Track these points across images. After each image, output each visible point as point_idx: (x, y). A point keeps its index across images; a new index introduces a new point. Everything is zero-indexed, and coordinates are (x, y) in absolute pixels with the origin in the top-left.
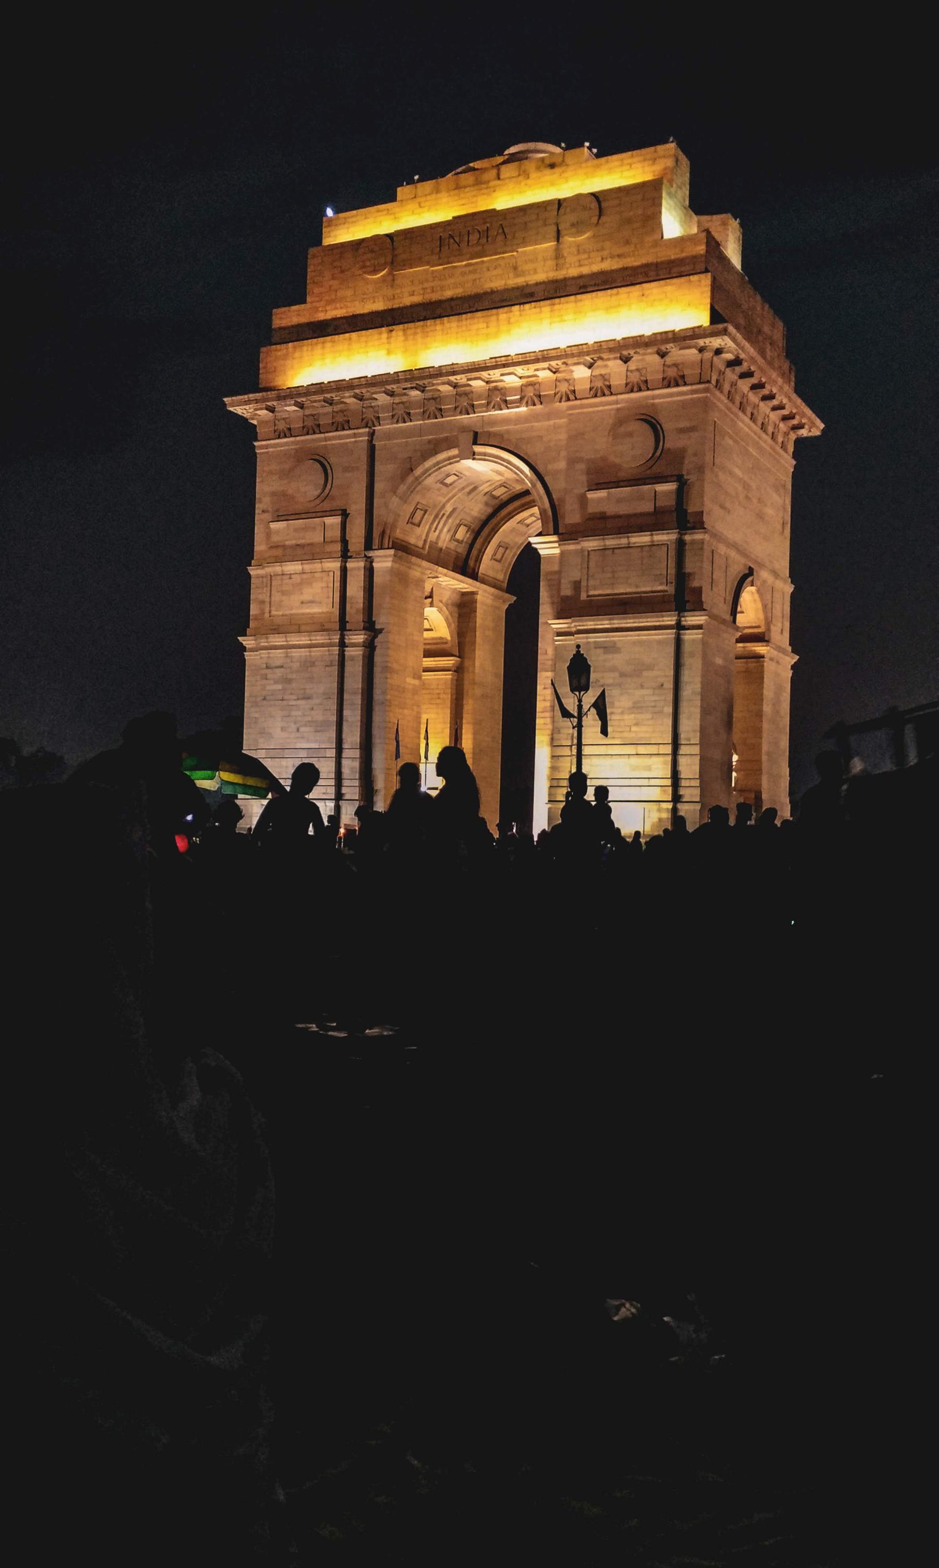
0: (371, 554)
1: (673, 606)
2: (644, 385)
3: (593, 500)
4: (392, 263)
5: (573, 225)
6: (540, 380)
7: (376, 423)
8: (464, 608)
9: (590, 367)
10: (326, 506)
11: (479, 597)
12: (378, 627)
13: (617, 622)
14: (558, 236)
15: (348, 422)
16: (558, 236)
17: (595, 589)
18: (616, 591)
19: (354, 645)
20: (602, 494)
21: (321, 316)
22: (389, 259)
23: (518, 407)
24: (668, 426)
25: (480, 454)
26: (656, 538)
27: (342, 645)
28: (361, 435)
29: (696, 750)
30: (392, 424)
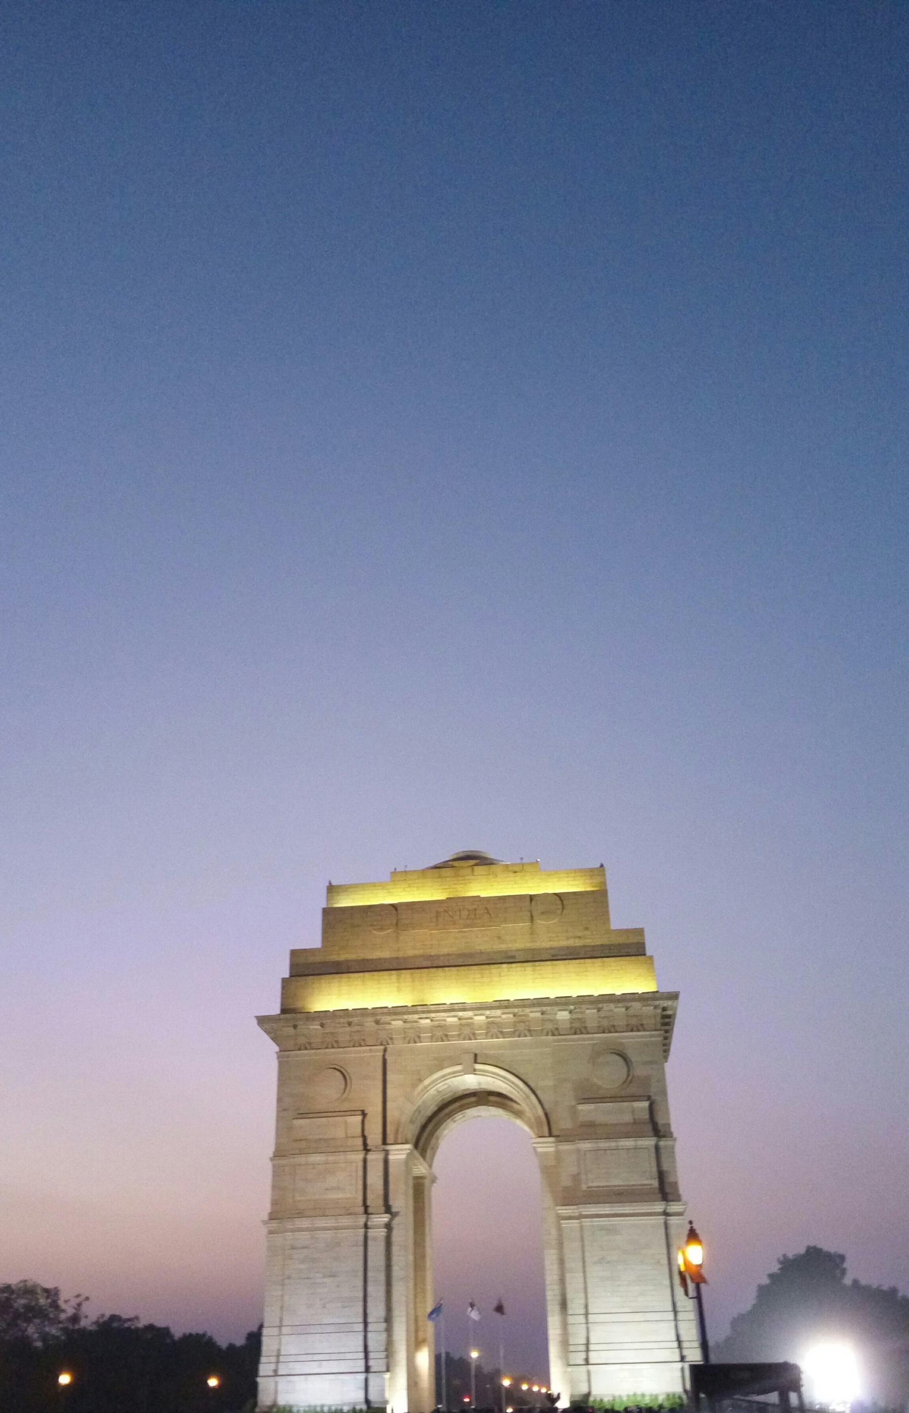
0: (389, 1147)
1: (660, 1196)
2: (612, 1029)
3: (582, 1110)
4: (397, 925)
5: (543, 913)
7: (390, 1041)
9: (570, 1012)
10: (346, 1106)
12: (394, 1210)
15: (364, 1040)
17: (593, 1182)
19: (376, 1227)
27: (366, 1226)
28: (378, 1051)
30: (403, 1043)
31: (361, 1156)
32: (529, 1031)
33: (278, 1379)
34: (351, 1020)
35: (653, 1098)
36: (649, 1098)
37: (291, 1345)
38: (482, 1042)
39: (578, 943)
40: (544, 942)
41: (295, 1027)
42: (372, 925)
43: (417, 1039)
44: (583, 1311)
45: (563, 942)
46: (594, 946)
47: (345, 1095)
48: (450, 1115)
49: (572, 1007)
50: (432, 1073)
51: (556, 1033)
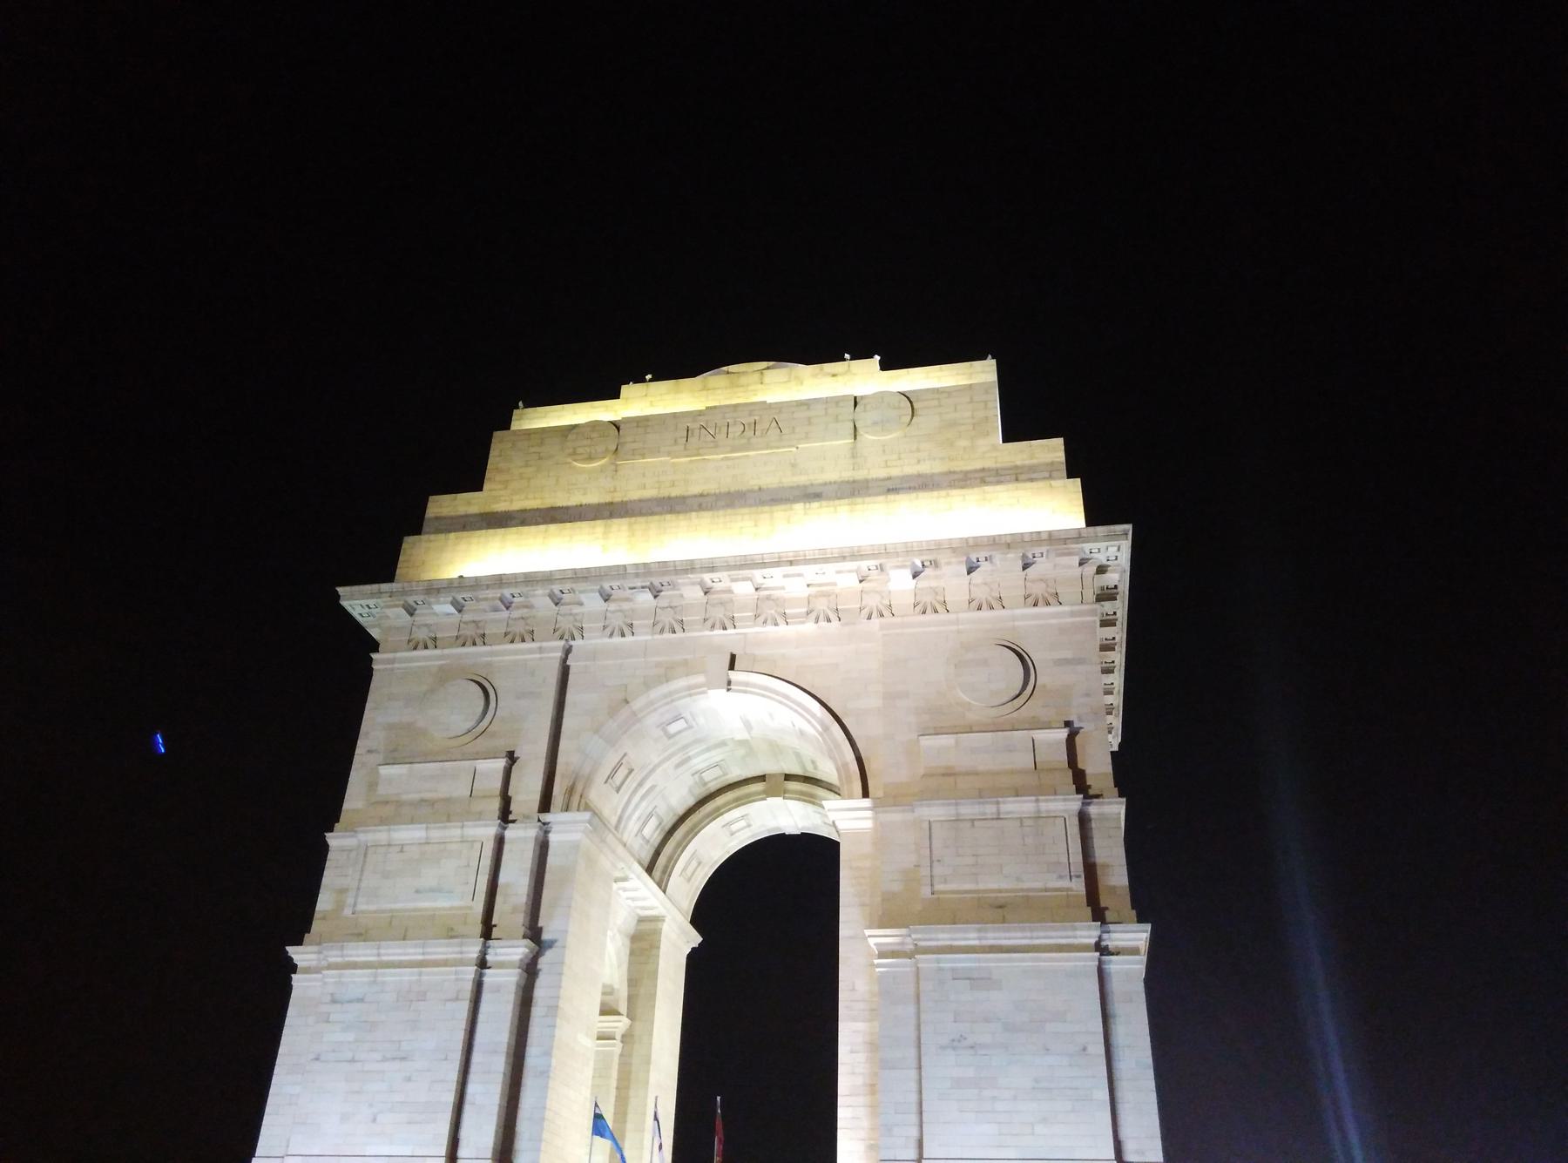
5: (875, 423)
6: (837, 590)
8: (643, 941)
11: (666, 928)
12: (545, 936)
13: (995, 937)
17: (945, 882)
18: (981, 886)
19: (501, 965)
20: (946, 740)
21: (501, 507)
26: (1044, 806)
27: (483, 964)
34: (507, 592)
36: (1068, 724)
43: (626, 630)
46: (966, 473)
48: (717, 813)
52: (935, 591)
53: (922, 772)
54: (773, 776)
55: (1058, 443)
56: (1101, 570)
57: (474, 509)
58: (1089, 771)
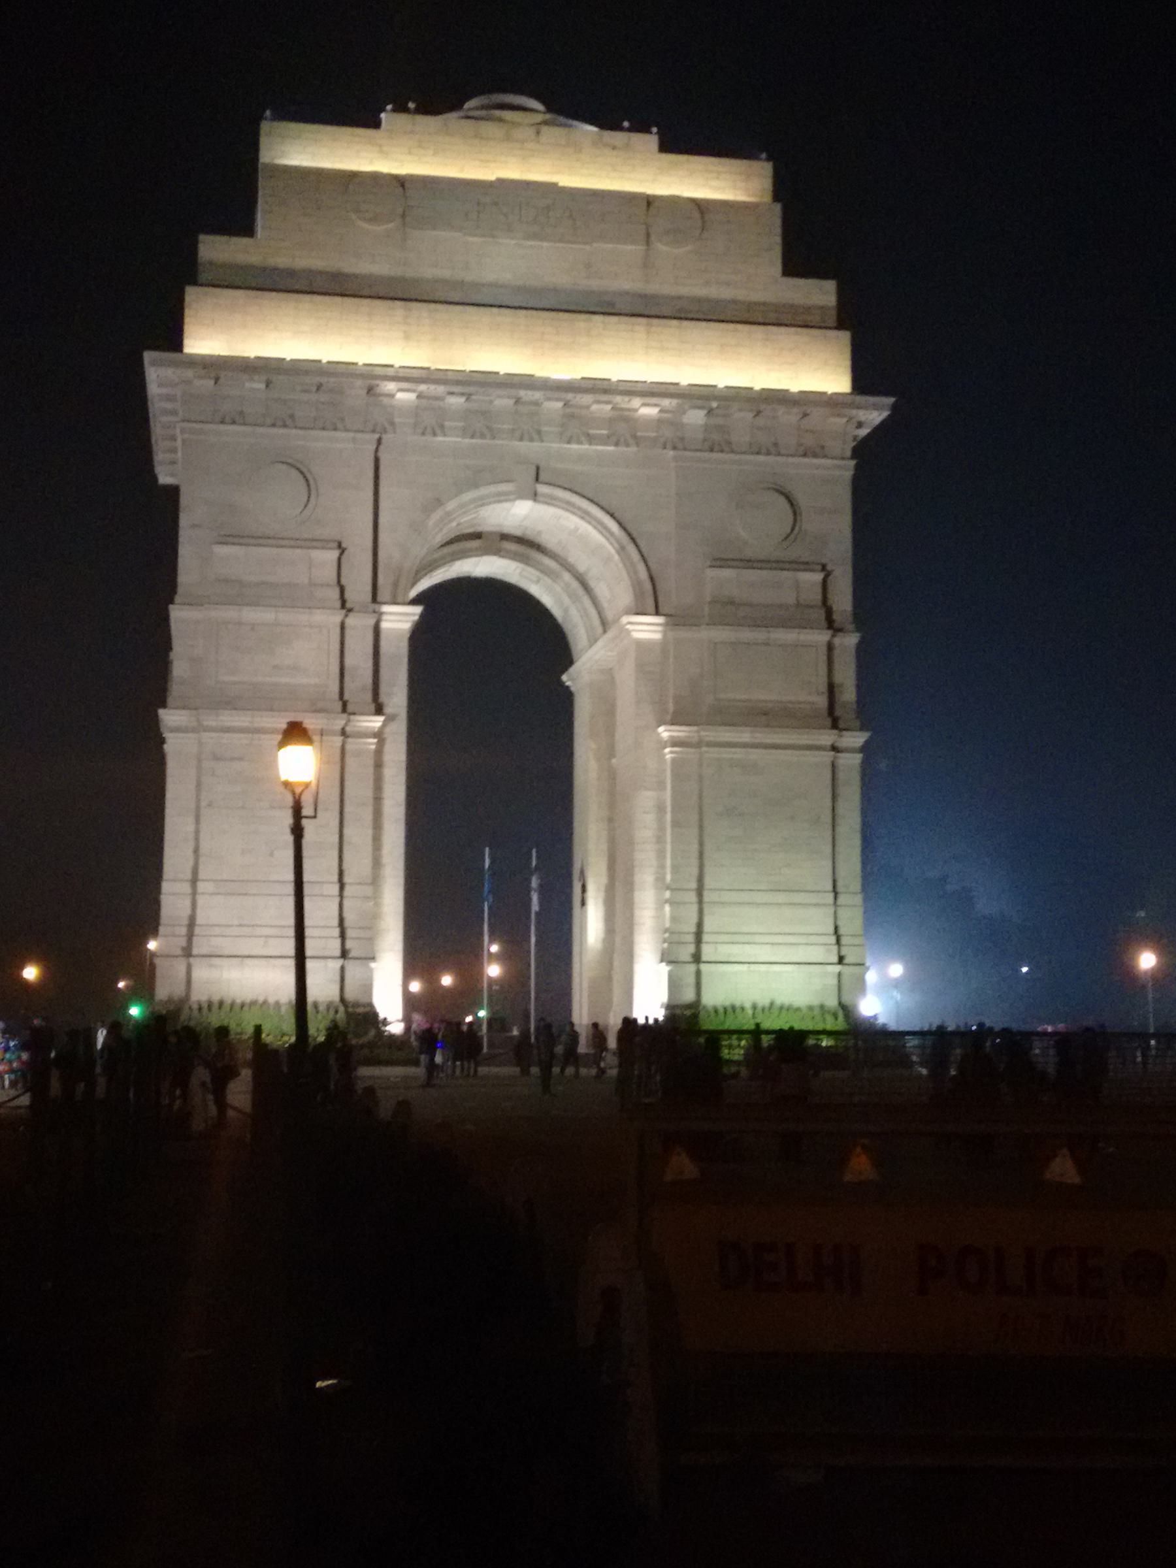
0: (386, 608)
1: (828, 722)
2: (775, 449)
4: (403, 216)
14: (648, 242)
15: (342, 420)
16: (648, 242)
20: (727, 573)
21: (282, 261)
22: (400, 210)
23: (606, 444)
24: (802, 501)
25: (544, 495)
27: (343, 733)
29: (859, 899)
31: (337, 618)
32: (634, 437)
33: (192, 960)
34: (324, 380)
35: (829, 568)
36: (824, 568)
37: (212, 910)
38: (547, 449)
39: (726, 293)
40: (665, 285)
41: (217, 380)
42: (357, 211)
43: (438, 431)
44: (694, 885)
45: (695, 289)
47: (307, 512)
49: (714, 404)
50: (460, 492)
51: (680, 445)
52: (720, 428)
53: (708, 599)
54: (491, 533)
55: (830, 286)
56: (860, 425)
57: (255, 259)
58: (835, 609)
